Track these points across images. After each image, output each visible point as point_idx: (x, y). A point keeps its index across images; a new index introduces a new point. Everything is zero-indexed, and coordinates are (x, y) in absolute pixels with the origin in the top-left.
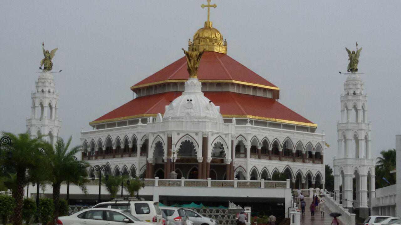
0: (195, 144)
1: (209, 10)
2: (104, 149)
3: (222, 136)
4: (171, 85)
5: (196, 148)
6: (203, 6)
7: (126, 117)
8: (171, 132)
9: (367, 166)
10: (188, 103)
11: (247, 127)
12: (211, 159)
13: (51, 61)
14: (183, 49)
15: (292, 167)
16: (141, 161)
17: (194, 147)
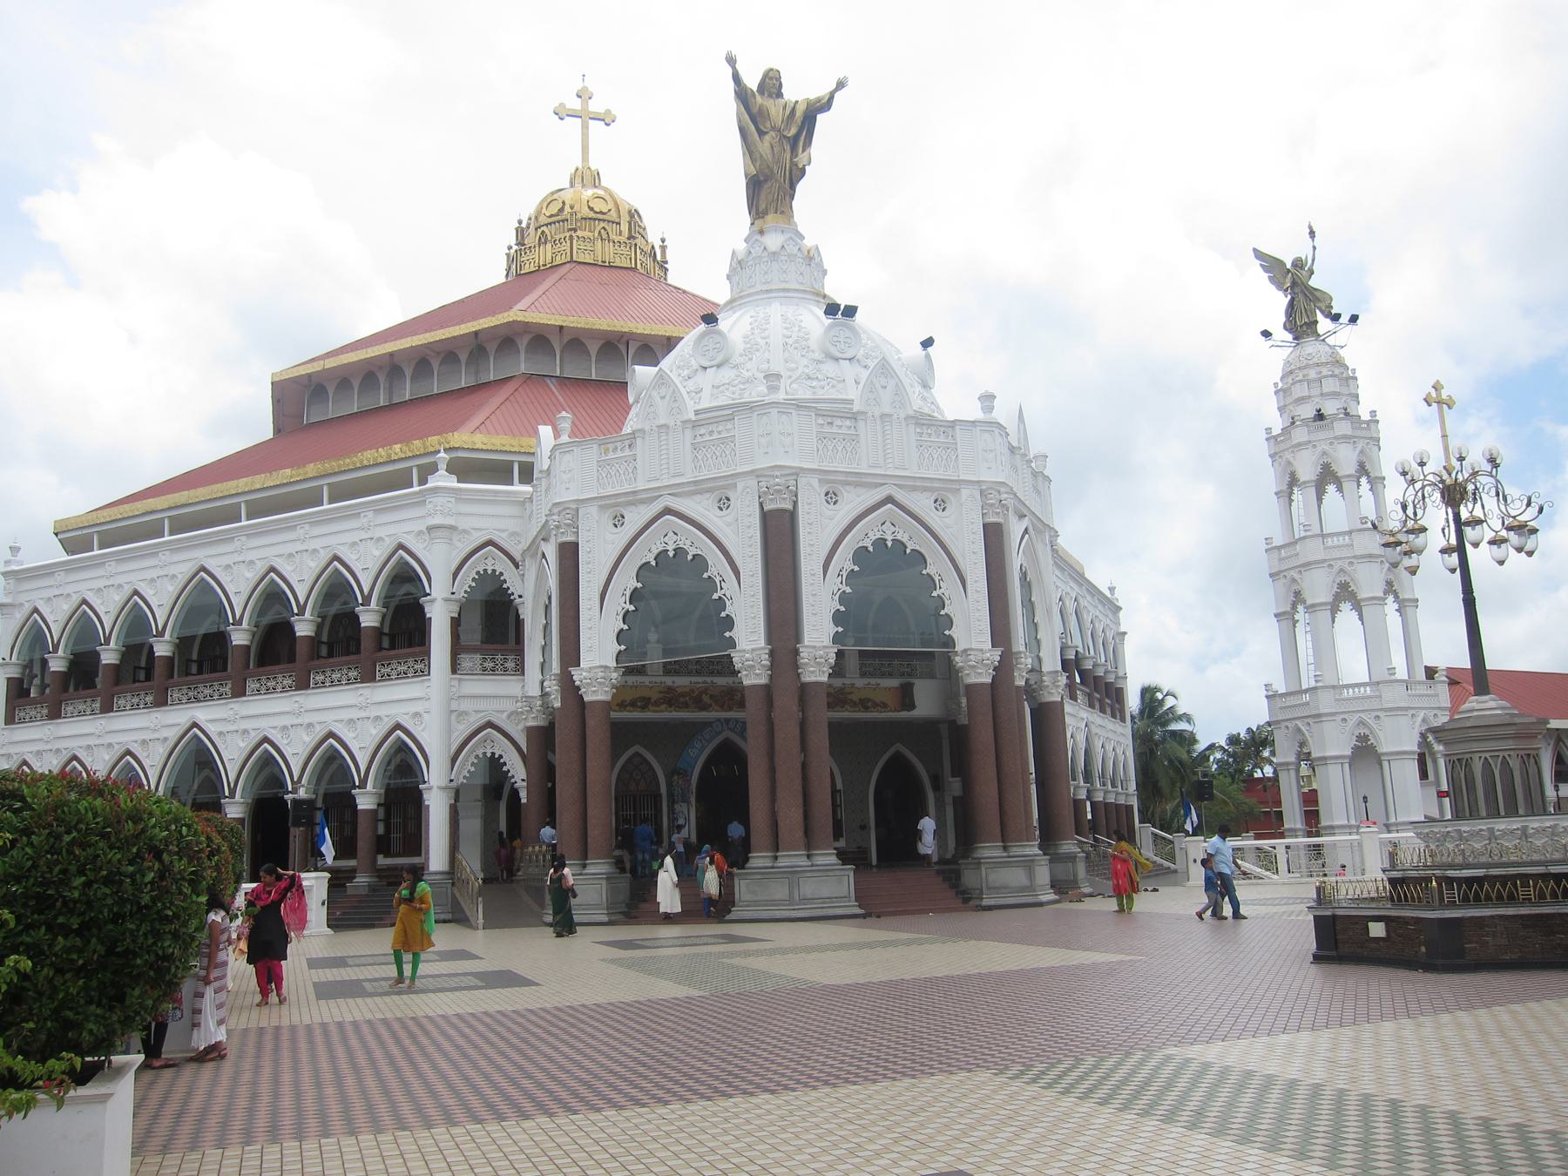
1: (585, 127)
2: (162, 649)
4: (523, 343)
6: (561, 113)
7: (311, 469)
8: (797, 473)
10: (831, 327)
14: (731, 61)
16: (454, 706)
17: (931, 583)
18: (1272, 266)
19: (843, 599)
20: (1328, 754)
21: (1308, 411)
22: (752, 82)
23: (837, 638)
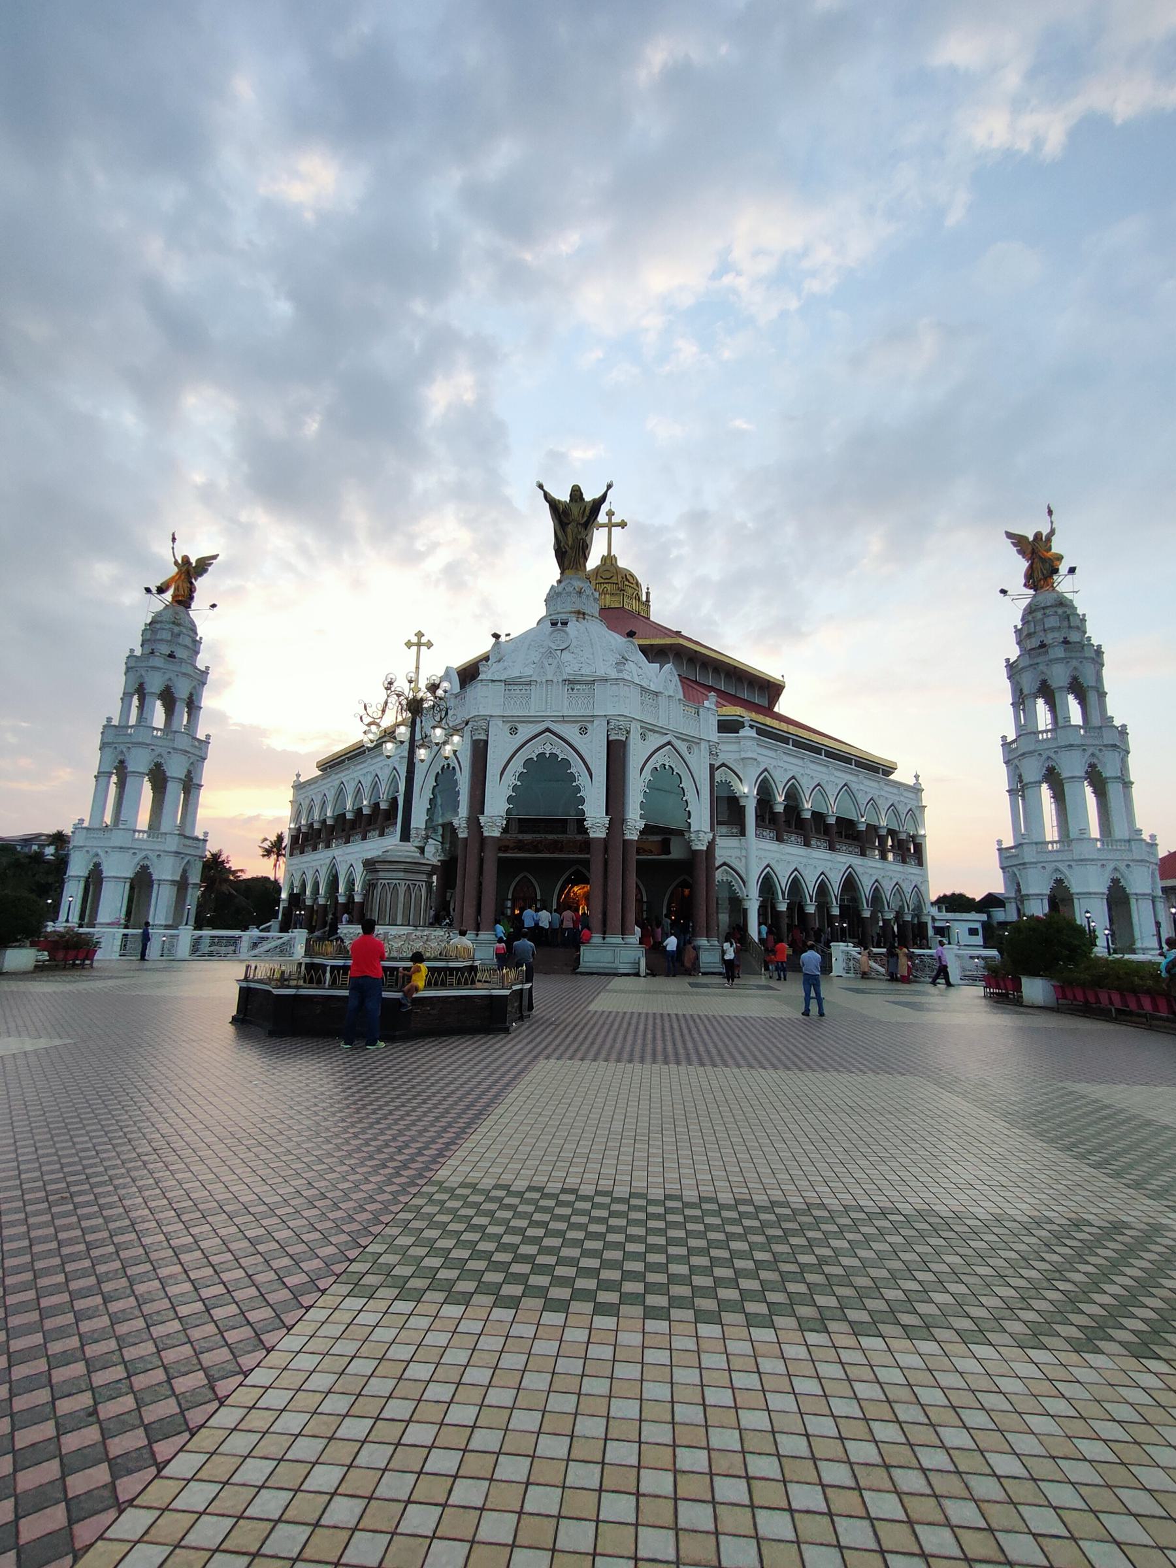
0: (577, 767)
3: (676, 743)
5: (583, 780)
8: (488, 719)
9: (1100, 863)
10: (553, 632)
11: (745, 737)
12: (641, 825)
13: (191, 583)
15: (859, 870)
17: (572, 778)
18: (1019, 541)
19: (515, 788)
20: (1092, 890)
21: (1034, 643)
22: (564, 496)
23: (508, 812)
